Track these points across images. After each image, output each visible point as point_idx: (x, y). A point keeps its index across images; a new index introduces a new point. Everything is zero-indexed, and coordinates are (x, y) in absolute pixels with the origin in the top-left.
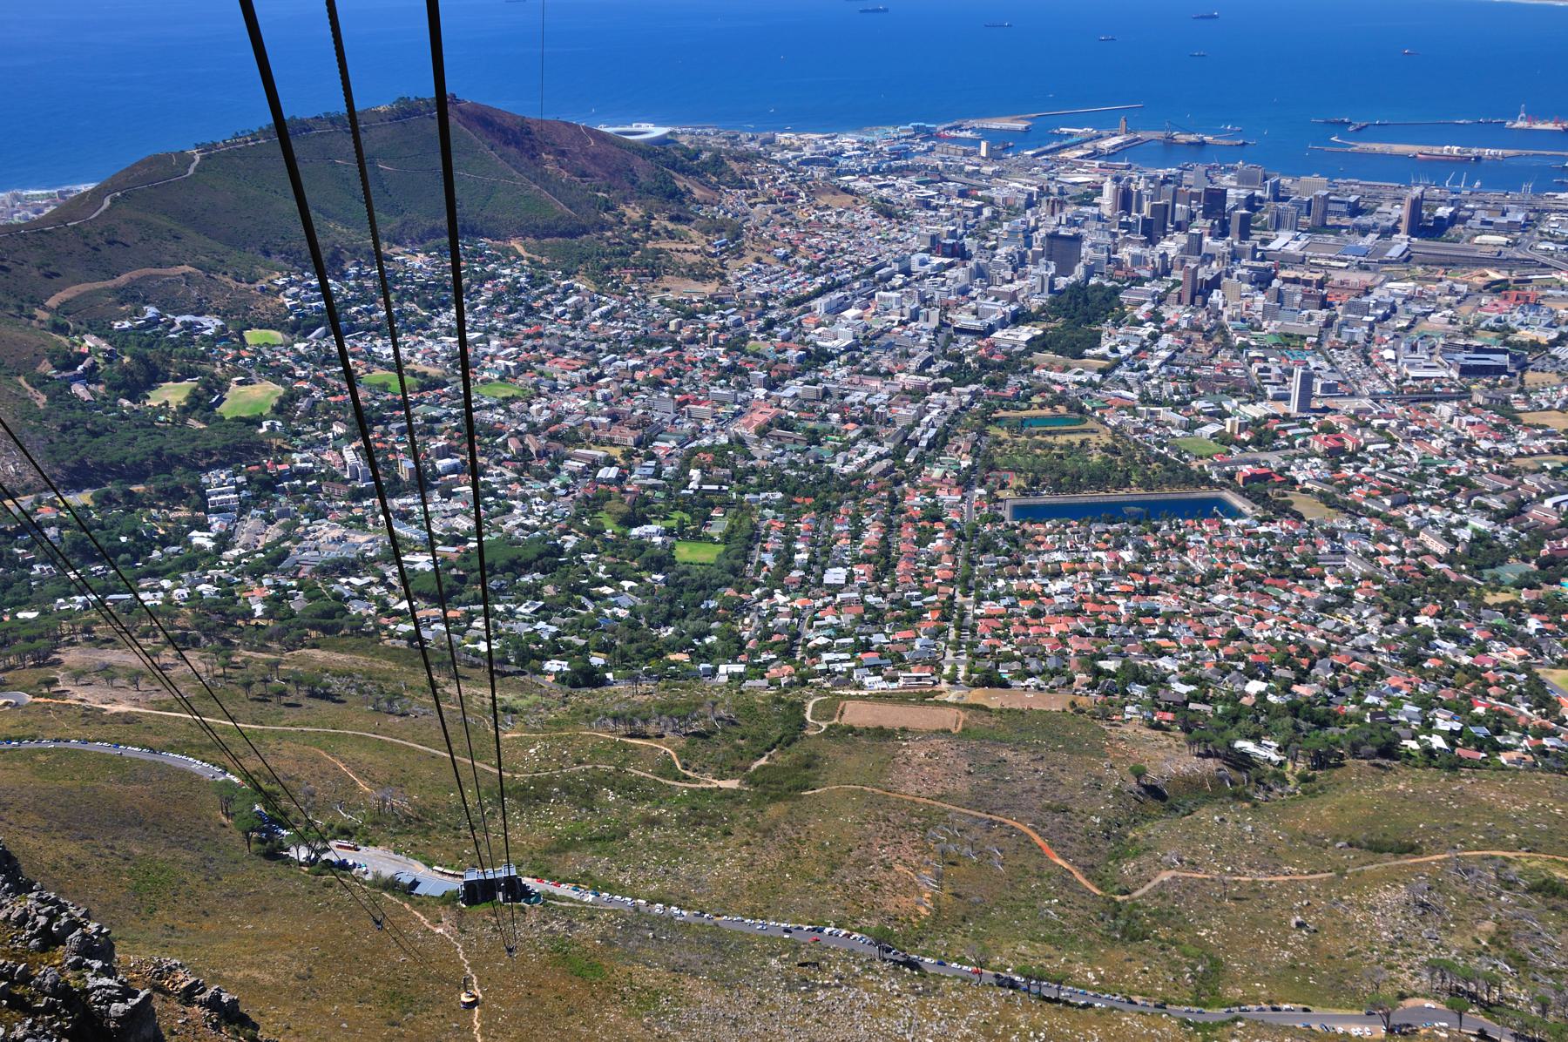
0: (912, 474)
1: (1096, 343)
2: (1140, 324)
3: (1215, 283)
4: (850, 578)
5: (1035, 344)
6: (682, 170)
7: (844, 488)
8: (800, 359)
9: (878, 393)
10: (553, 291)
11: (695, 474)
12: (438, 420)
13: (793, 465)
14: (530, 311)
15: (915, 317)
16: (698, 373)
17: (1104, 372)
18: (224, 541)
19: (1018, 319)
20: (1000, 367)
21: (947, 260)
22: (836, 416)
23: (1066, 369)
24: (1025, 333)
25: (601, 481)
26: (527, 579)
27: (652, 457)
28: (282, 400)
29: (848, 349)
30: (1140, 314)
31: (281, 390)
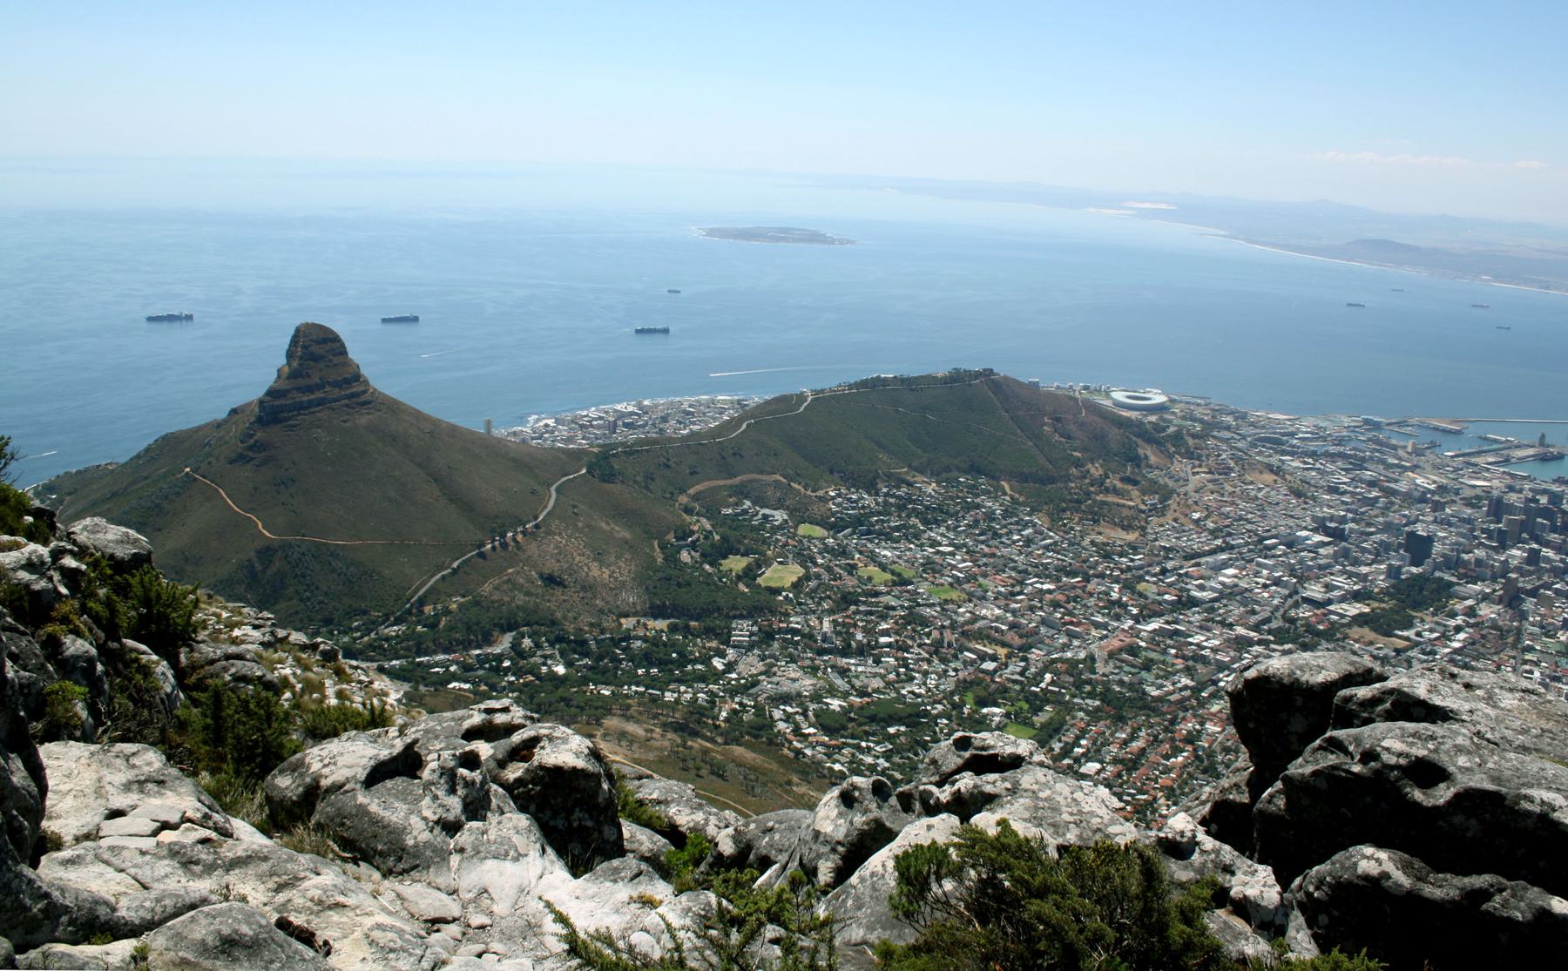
0: (1202, 704)
1: (1409, 626)
2: (1453, 615)
3: (1533, 593)
4: (1098, 772)
5: (1360, 620)
6: (1149, 441)
7: (1146, 707)
8: (1172, 603)
9: (1208, 641)
10: (1017, 523)
11: (1048, 677)
12: (894, 608)
13: (1121, 683)
14: (996, 535)
15: (1277, 582)
16: (1092, 601)
17: (1398, 651)
18: (730, 667)
19: (1356, 597)
20: (1318, 634)
21: (1327, 539)
22: (1173, 651)
23: (1371, 643)
24: (1353, 609)
25: (984, 671)
26: (892, 730)
27: (1025, 659)
28: (800, 579)
29: (1214, 600)
30: (1459, 607)
31: (801, 571)
